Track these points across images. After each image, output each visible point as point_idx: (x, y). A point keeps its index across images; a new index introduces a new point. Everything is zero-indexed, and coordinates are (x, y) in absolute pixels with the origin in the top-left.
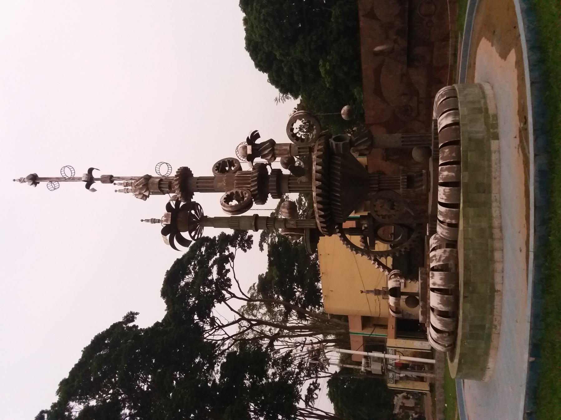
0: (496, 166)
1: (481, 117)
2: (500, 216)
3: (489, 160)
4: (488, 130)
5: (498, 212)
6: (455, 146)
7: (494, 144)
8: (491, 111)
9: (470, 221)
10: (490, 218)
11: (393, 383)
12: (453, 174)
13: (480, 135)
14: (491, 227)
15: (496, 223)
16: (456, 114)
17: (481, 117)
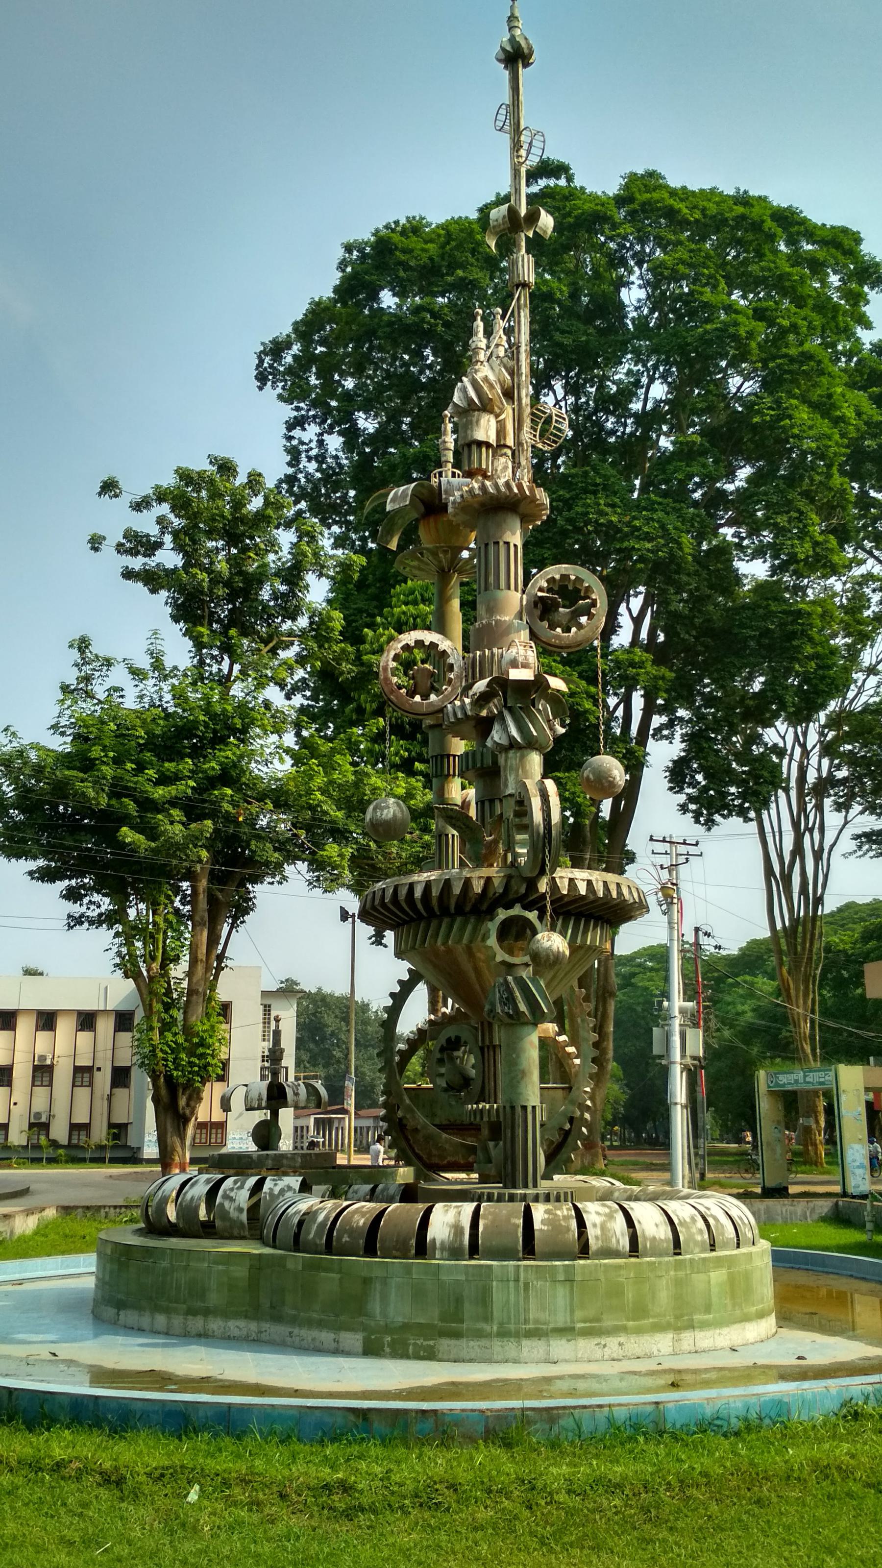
0: (310, 1339)
1: (431, 1315)
2: (229, 1338)
3: (321, 1325)
4: (387, 1329)
5: (237, 1333)
6: (362, 1242)
7: (353, 1339)
8: (444, 1344)
9: (221, 1267)
10: (226, 1314)
11: (769, 1087)
12: (311, 1236)
13: (376, 1307)
14: (207, 1312)
15: (215, 1325)
16: (454, 1252)
17: (431, 1315)
